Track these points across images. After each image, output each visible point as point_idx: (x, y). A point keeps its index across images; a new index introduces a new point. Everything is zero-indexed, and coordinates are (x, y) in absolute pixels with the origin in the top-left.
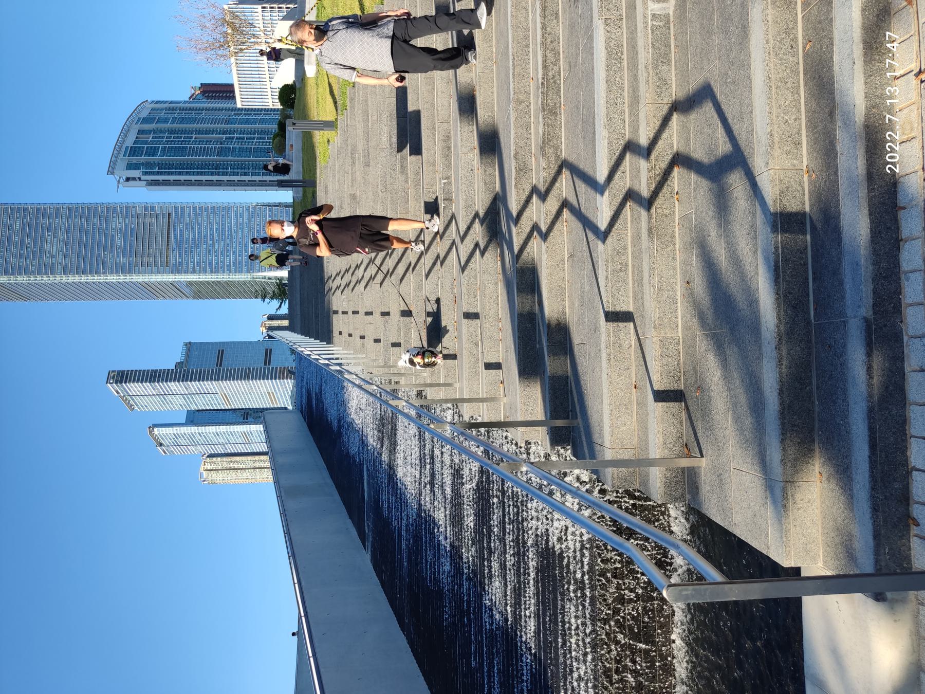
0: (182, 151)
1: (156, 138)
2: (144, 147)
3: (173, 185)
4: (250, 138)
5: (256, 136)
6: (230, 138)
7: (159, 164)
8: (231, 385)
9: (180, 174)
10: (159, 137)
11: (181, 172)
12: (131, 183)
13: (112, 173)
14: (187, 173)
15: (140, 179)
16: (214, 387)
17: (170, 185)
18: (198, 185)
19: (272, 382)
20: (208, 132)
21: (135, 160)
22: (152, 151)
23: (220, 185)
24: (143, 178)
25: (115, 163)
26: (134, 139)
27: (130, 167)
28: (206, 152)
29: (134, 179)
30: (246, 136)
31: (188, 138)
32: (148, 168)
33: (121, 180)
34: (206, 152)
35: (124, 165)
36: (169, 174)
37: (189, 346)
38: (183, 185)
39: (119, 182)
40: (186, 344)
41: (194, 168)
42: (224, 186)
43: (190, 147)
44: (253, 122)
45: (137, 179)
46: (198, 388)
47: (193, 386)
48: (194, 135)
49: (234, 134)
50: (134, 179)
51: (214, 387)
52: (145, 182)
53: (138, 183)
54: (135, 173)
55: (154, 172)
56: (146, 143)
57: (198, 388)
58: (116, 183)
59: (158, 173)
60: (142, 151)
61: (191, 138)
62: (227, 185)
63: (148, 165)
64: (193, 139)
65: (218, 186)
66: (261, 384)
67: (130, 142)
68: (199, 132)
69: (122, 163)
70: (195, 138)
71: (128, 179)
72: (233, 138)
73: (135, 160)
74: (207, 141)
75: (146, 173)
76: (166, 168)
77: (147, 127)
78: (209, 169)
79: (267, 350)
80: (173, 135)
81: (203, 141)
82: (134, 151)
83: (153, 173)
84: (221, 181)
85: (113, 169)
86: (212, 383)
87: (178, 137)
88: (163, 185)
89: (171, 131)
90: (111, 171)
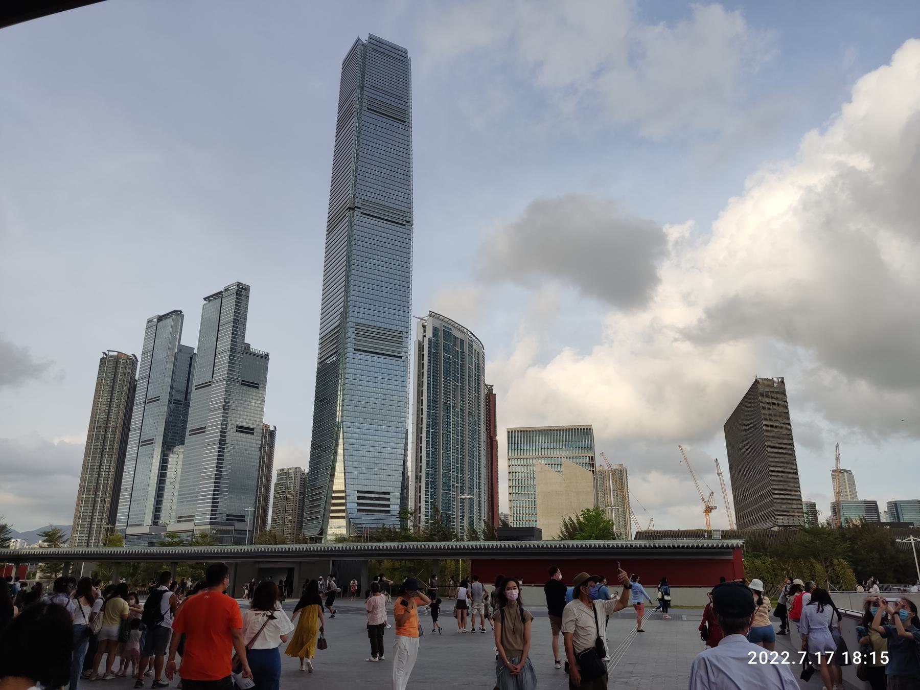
0: (447, 373)
1: (458, 353)
2: (451, 343)
3: (419, 363)
5: (460, 438)
7: (438, 353)
8: (221, 392)
9: (429, 369)
10: (458, 356)
12: (421, 329)
13: (430, 315)
14: (429, 375)
15: (424, 336)
16: (220, 376)
17: (419, 360)
18: (418, 384)
19: (217, 432)
20: (463, 396)
21: (441, 334)
22: (446, 350)
23: (418, 402)
24: (426, 339)
25: (438, 318)
26: (457, 336)
27: (435, 330)
28: (447, 394)
29: (424, 332)
31: (458, 379)
32: (434, 344)
33: (423, 322)
34: (447, 394)
35: (437, 326)
36: (429, 360)
37: (266, 357)
38: (419, 371)
39: (421, 319)
40: (266, 357)
41: (433, 382)
42: (417, 406)
43: (450, 389)
44: (471, 437)
45: (424, 334)
46: (222, 361)
47: (225, 356)
48: (460, 384)
50: (424, 332)
51: (220, 376)
52: (422, 340)
53: (421, 335)
54: (429, 333)
55: (431, 348)
56: (454, 345)
57: (222, 361)
58: (421, 317)
59: (429, 351)
60: (447, 341)
62: (417, 408)
63: (437, 345)
64: (457, 384)
65: (418, 401)
66: (217, 421)
67: (454, 332)
68: (462, 388)
69: (438, 324)
71: (424, 327)
73: (441, 334)
74: (455, 395)
75: (430, 341)
76: (434, 357)
77: (466, 347)
78: (433, 394)
79: (253, 429)
81: (455, 392)
82: (447, 334)
83: (429, 347)
84: (422, 403)
85: (434, 316)
86: (225, 374)
87: (458, 371)
88: (419, 354)
89: (462, 366)
90: (431, 314)
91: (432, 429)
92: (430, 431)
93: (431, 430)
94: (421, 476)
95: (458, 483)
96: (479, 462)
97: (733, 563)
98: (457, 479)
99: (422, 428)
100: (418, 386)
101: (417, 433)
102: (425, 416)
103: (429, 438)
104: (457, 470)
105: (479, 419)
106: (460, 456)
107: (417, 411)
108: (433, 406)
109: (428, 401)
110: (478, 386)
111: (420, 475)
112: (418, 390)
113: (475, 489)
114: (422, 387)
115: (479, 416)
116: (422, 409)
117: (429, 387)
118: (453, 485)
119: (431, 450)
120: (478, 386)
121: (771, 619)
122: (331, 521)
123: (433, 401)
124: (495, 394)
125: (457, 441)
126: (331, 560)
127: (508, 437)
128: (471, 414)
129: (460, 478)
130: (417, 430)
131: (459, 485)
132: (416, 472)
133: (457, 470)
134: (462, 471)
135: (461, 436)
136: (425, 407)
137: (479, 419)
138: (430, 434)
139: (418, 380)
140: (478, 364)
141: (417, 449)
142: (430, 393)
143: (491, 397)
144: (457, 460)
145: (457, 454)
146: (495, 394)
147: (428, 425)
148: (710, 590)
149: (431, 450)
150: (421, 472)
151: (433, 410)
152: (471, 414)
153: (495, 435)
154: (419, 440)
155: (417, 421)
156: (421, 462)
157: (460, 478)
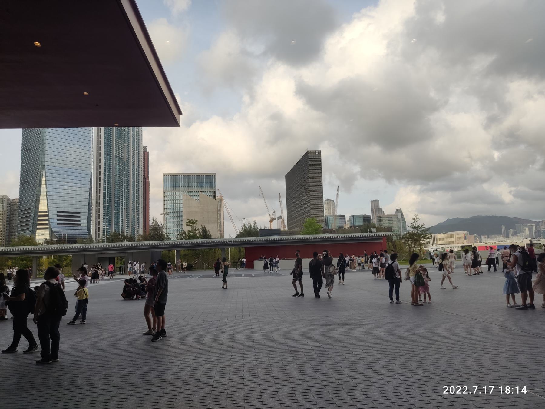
4: (125, 175)
6: (125, 164)
11: (106, 134)
14: (105, 137)
18: (97, 142)
20: (128, 152)
23: (97, 155)
28: (118, 149)
30: (126, 173)
34: (118, 149)
38: (98, 134)
41: (108, 142)
43: (120, 147)
48: (126, 144)
49: (127, 166)
61: (125, 143)
62: (97, 159)
64: (124, 144)
70: (124, 145)
72: (125, 166)
80: (126, 133)
84: (100, 155)
87: (125, 136)
91: (108, 172)
92: (106, 174)
93: (107, 173)
94: (99, 202)
95: (125, 207)
96: (138, 194)
97: (382, 244)
98: (124, 205)
99: (100, 171)
100: (97, 144)
101: (97, 175)
102: (102, 164)
103: (106, 178)
104: (124, 199)
105: (138, 167)
106: (126, 190)
107: (97, 161)
108: (108, 158)
109: (105, 154)
110: (138, 146)
111: (99, 201)
112: (97, 146)
113: (136, 210)
114: (100, 145)
115: (139, 165)
116: (100, 159)
117: (105, 145)
118: (121, 208)
119: (107, 186)
120: (138, 146)
121: (447, 264)
122: (38, 231)
123: (109, 154)
124: (148, 152)
125: (125, 181)
126: (150, 250)
127: (215, 182)
128: (133, 164)
129: (126, 204)
130: (97, 173)
131: (126, 208)
132: (96, 200)
133: (124, 199)
134: (128, 200)
135: (127, 178)
136: (102, 158)
137: (138, 167)
138: (106, 176)
139: (97, 140)
140: (138, 132)
141: (96, 185)
142: (106, 149)
143: (146, 154)
144: (125, 193)
145: (125, 189)
146: (148, 152)
147: (105, 170)
148: (295, 260)
149: (107, 186)
150: (99, 200)
151: (108, 160)
152: (133, 164)
153: (148, 178)
154: (98, 179)
155: (97, 167)
156: (100, 193)
157: (126, 204)
